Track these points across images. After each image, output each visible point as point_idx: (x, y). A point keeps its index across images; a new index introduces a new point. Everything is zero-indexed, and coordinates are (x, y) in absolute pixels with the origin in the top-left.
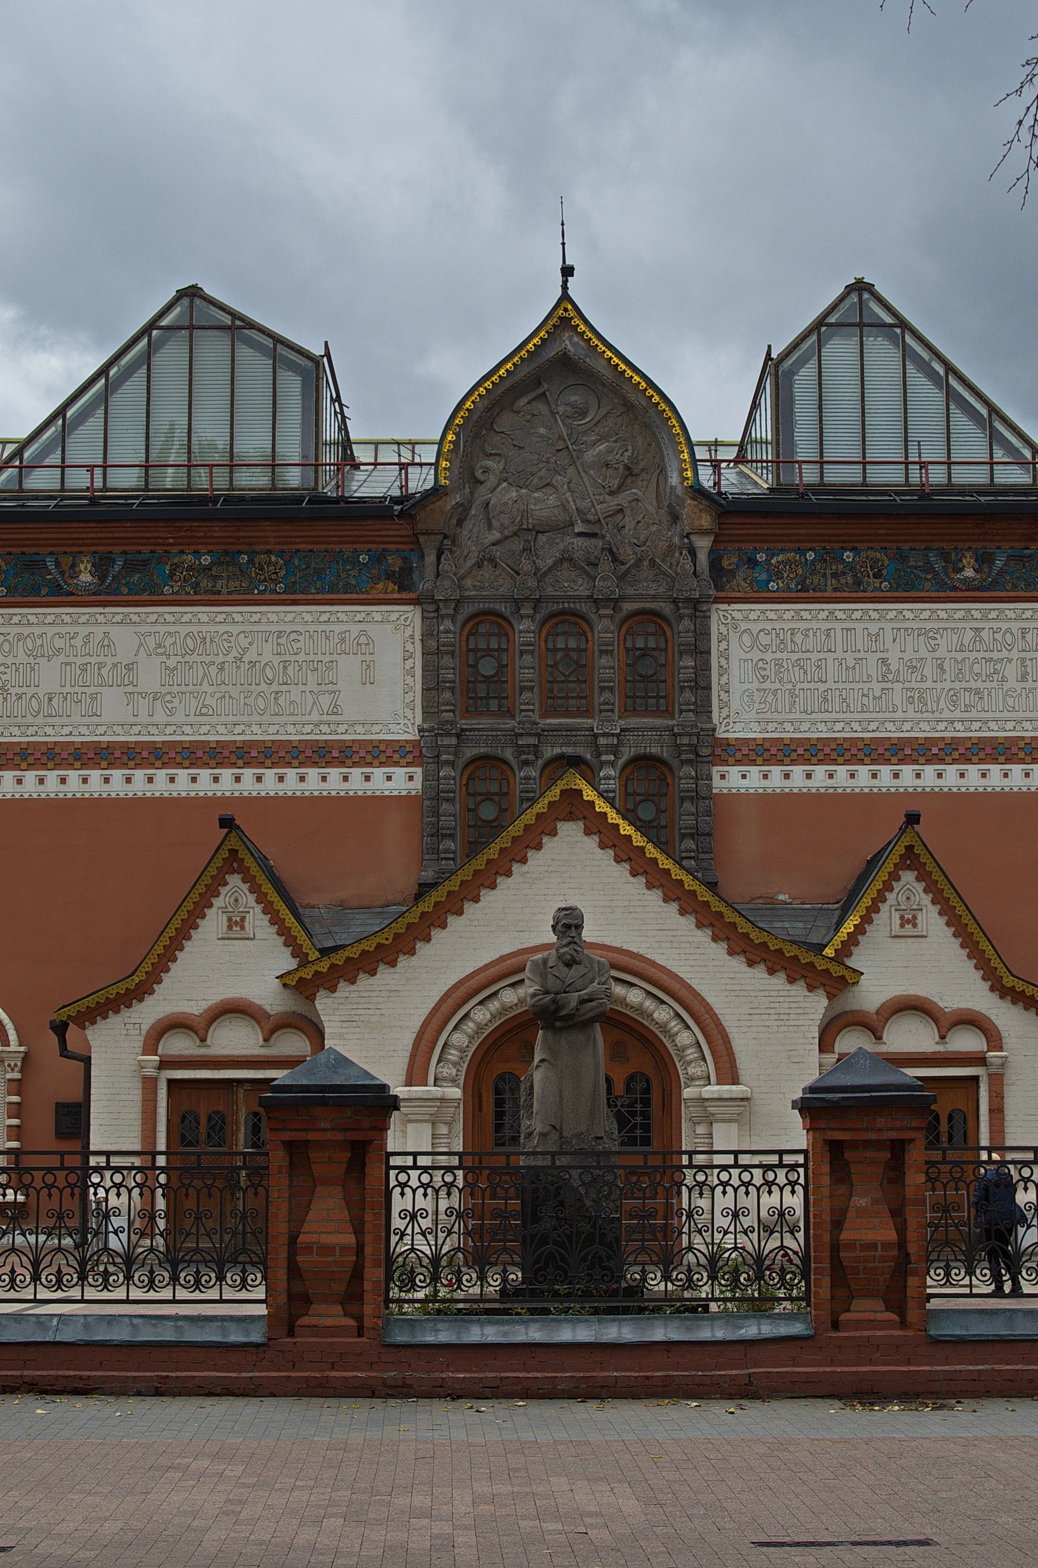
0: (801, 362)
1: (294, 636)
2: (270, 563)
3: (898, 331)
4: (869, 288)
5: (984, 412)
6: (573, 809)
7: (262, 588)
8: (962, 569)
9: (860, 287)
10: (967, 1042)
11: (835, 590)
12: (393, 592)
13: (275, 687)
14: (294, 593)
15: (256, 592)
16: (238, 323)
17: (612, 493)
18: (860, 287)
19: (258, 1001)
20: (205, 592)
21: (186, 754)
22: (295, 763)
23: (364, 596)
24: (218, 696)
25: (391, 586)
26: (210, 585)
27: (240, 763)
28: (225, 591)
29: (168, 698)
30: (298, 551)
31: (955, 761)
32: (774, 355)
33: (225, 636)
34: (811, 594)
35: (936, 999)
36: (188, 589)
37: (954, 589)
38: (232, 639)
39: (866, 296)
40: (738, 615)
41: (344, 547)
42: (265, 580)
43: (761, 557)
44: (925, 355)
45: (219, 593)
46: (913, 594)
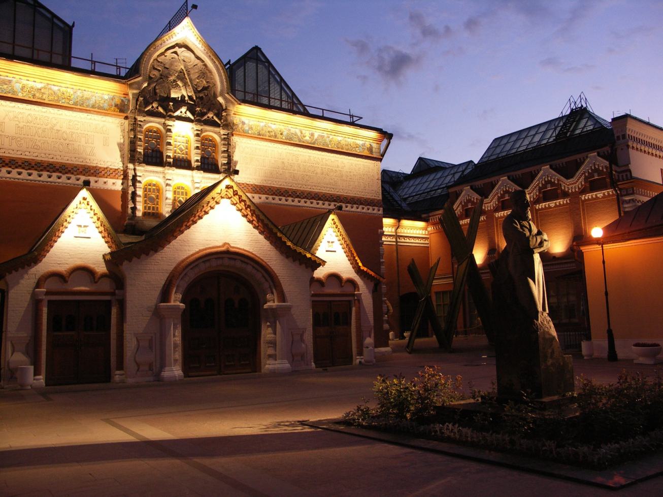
0: (239, 67)
1: (76, 123)
2: (67, 92)
3: (266, 64)
4: (260, 49)
5: (290, 94)
6: (228, 193)
7: (63, 101)
8: (305, 137)
9: (256, 49)
10: (348, 289)
11: (269, 136)
12: (117, 112)
13: (67, 142)
14: (77, 105)
15: (61, 102)
16: (36, 5)
17: (200, 92)
18: (256, 49)
19: (92, 266)
20: (38, 99)
21: (26, 164)
22: (75, 173)
23: (106, 112)
24: (42, 141)
25: (117, 110)
26: (40, 96)
27: (51, 170)
28: (47, 99)
29: (19, 139)
30: (79, 89)
31: (304, 198)
32: (231, 63)
33: (46, 118)
34: (261, 137)
35: (339, 273)
36: (30, 96)
37: (304, 142)
38: (49, 120)
39: (259, 51)
40: (238, 140)
41: (99, 92)
42: (65, 98)
43: (246, 122)
44: (274, 73)
45: (44, 100)
46: (292, 142)
